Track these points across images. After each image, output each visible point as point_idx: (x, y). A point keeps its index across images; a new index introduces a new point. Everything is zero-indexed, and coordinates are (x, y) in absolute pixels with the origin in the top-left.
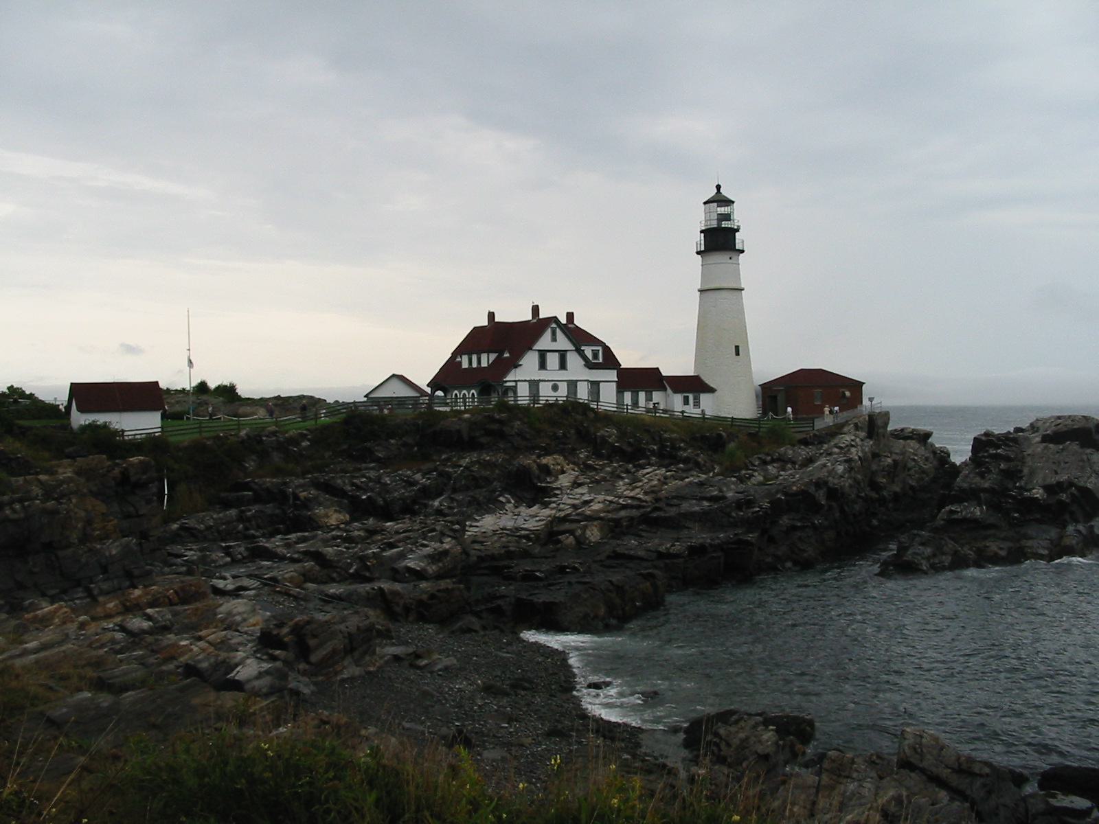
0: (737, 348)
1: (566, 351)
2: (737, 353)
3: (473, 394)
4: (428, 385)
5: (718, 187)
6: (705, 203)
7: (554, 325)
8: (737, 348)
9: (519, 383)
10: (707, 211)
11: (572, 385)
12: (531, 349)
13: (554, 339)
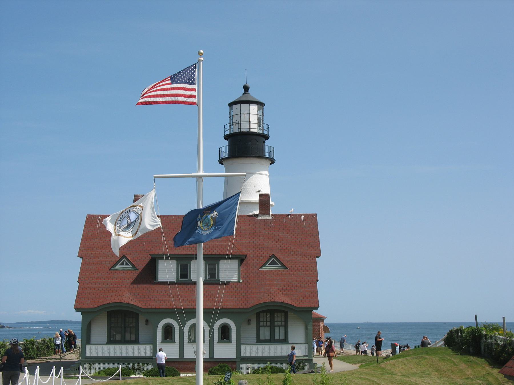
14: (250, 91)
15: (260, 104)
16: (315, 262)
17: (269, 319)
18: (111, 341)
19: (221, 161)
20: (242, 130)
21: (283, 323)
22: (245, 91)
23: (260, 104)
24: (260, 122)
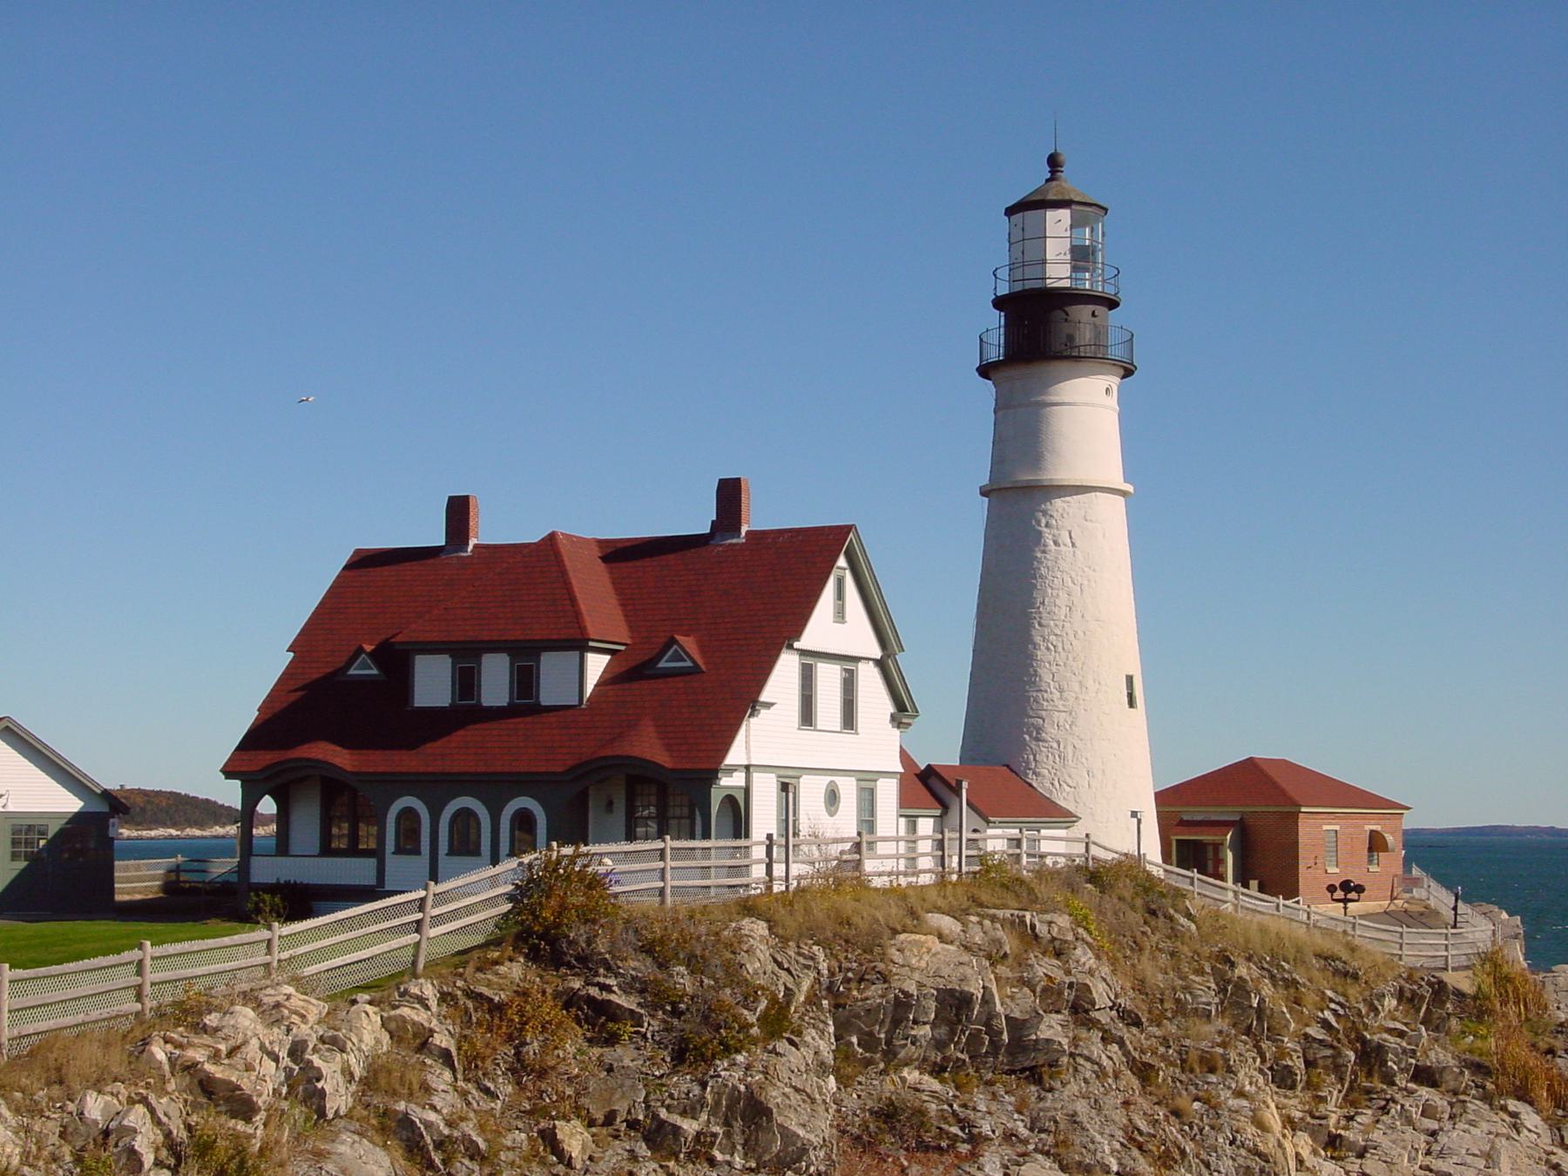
0: (1130, 679)
1: (857, 659)
2: (1131, 696)
3: (524, 821)
4: (229, 772)
5: (1054, 162)
6: (1010, 212)
7: (842, 562)
8: (1130, 679)
9: (757, 777)
10: (1017, 235)
11: (867, 782)
12: (790, 647)
13: (840, 615)
14: (1066, 173)
15: (1086, 210)
16: (777, 656)
17: (653, 799)
18: (327, 850)
19: (985, 371)
20: (1029, 285)
21: (686, 811)
22: (1053, 172)
23: (1086, 210)
24: (1081, 256)
